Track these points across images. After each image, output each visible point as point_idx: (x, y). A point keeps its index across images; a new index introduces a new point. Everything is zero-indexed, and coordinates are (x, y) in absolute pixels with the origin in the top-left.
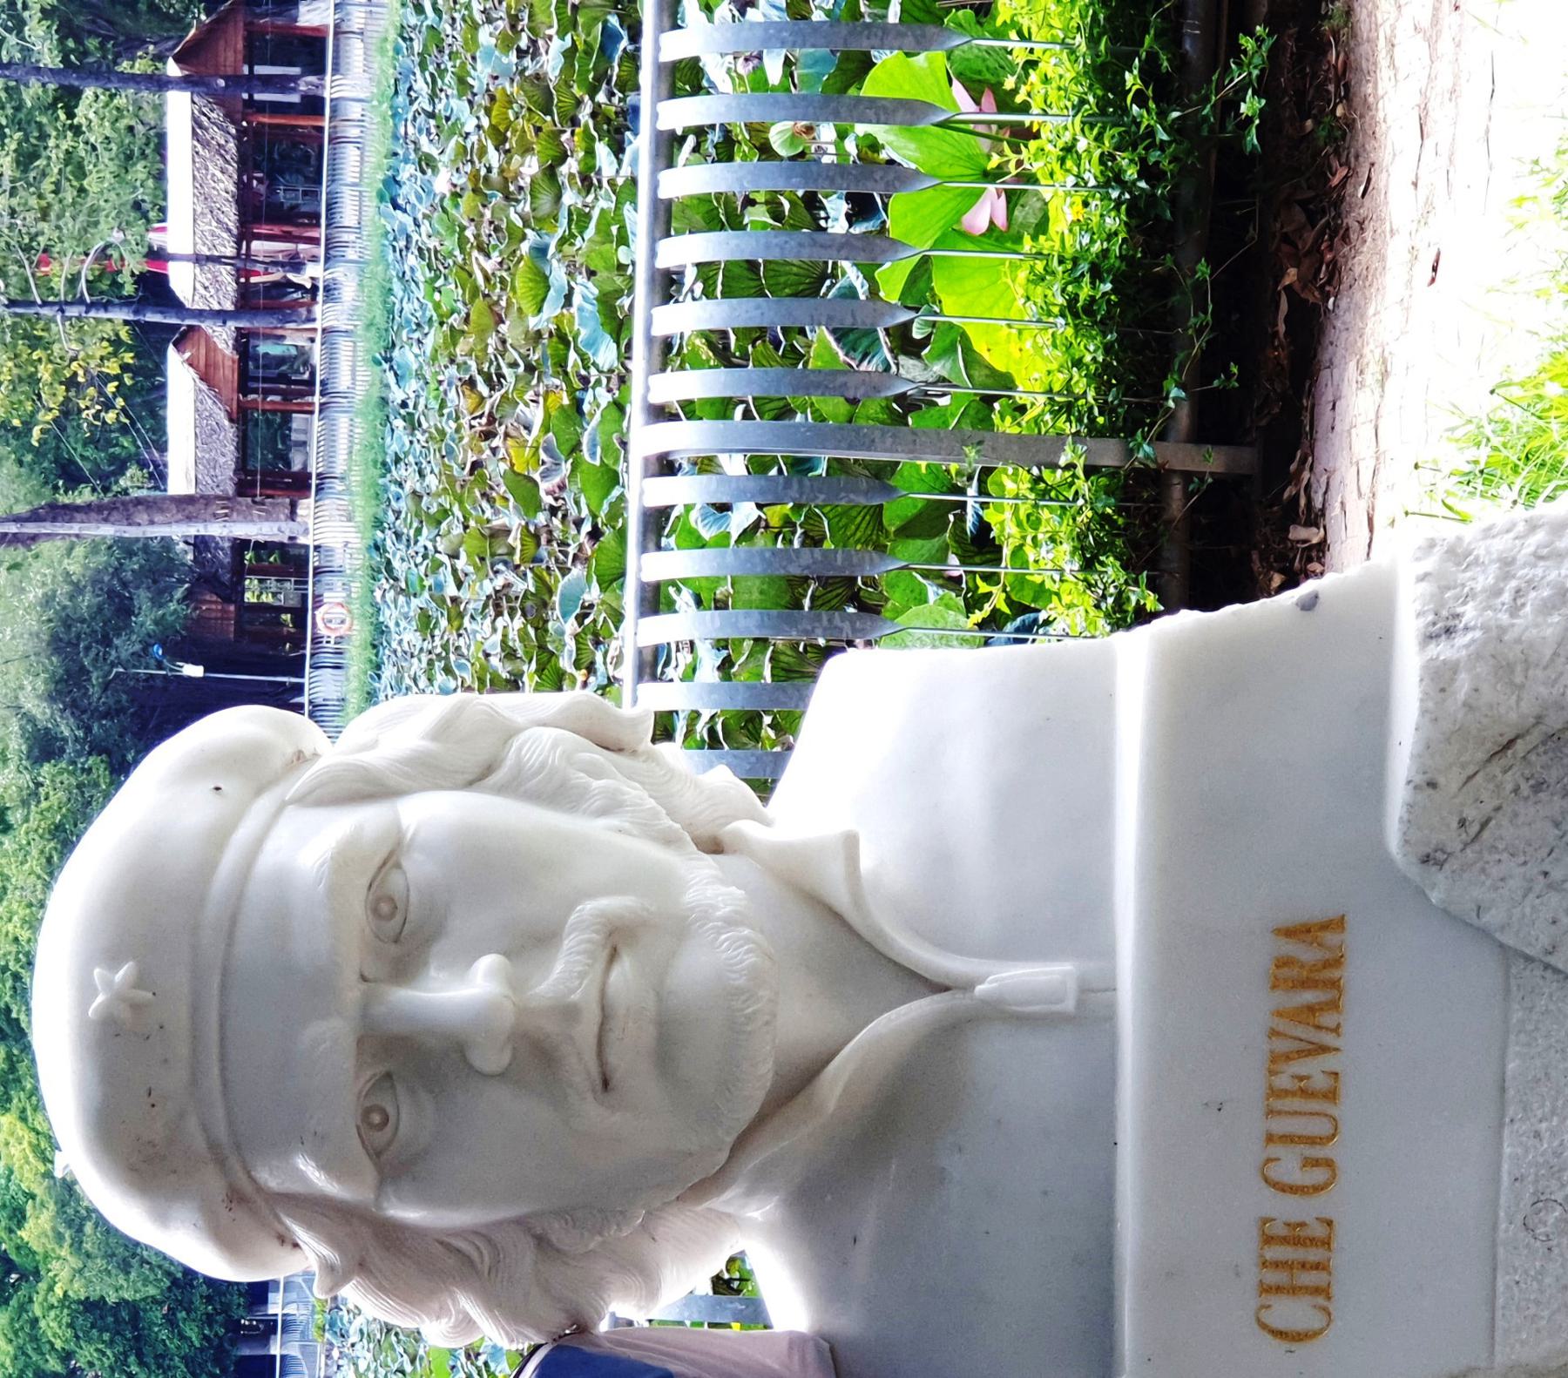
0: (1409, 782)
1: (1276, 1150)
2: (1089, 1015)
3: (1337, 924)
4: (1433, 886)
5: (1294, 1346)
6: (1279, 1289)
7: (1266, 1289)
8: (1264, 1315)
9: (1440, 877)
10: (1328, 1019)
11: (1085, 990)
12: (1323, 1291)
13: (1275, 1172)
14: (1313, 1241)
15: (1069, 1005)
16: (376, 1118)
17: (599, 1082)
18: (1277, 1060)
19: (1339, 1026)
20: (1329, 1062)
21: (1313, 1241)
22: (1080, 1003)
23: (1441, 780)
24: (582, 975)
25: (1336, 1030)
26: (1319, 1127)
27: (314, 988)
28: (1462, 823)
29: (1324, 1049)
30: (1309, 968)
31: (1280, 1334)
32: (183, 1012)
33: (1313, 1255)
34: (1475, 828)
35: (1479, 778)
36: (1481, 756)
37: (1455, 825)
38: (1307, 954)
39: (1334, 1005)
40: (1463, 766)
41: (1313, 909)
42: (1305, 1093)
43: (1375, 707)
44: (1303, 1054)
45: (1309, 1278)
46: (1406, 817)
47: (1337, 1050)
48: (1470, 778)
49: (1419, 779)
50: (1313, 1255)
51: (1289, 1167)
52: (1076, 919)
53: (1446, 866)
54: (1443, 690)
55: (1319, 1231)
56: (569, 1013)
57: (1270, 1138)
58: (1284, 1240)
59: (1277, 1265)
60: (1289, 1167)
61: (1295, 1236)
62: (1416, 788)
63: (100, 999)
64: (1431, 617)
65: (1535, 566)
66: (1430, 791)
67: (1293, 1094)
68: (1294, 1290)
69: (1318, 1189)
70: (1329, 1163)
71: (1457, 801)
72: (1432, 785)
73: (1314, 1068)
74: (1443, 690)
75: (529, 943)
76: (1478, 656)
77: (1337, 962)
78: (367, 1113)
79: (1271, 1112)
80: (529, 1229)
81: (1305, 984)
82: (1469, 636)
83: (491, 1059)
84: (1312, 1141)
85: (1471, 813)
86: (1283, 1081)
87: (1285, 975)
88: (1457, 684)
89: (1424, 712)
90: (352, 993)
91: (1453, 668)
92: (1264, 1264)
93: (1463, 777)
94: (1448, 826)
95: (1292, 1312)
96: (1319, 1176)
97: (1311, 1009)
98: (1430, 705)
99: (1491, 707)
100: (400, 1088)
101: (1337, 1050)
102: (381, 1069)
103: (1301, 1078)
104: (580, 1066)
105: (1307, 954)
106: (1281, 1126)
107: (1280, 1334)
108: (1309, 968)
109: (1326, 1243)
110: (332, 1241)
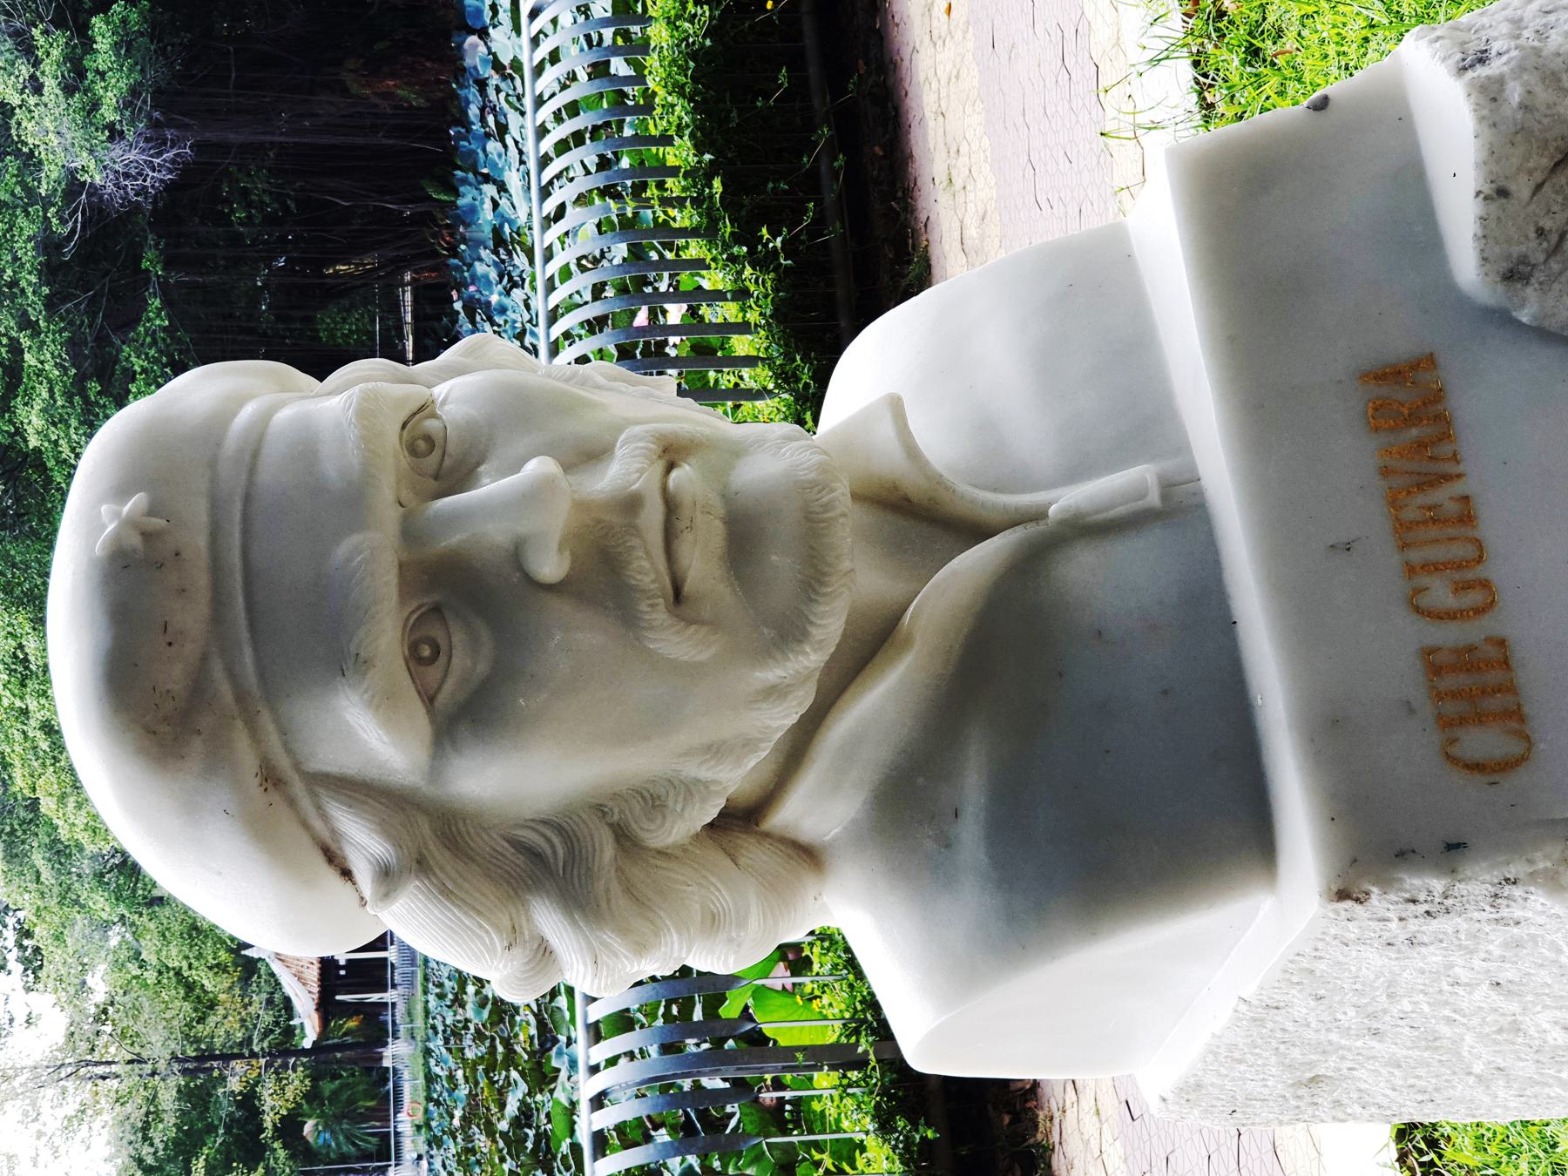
0: (1478, 194)
1: (1425, 580)
2: (1179, 511)
3: (1428, 361)
4: (1523, 303)
5: (1496, 778)
6: (1463, 721)
7: (1446, 723)
8: (1455, 750)
9: (1529, 290)
10: (1445, 449)
11: (1168, 487)
12: (1515, 715)
13: (1425, 601)
14: (1489, 664)
15: (1154, 499)
16: (426, 652)
17: (670, 592)
18: (1394, 502)
19: (1455, 455)
20: (1458, 488)
21: (1489, 664)
22: (1165, 496)
23: (1513, 187)
24: (641, 471)
25: (1455, 458)
26: (1458, 551)
27: (351, 503)
28: (1541, 232)
29: (1448, 478)
30: (1409, 408)
31: (1476, 767)
32: (202, 541)
33: (1494, 677)
34: (1554, 238)
35: (1547, 188)
36: (1546, 162)
37: (1532, 235)
38: (1402, 394)
39: (1446, 436)
40: (1530, 173)
41: (1399, 345)
42: (1434, 521)
43: (1410, 181)
44: (1420, 487)
45: (1495, 703)
46: (1480, 234)
47: (1459, 476)
48: (1539, 187)
49: (1487, 189)
50: (1494, 677)
51: (1440, 593)
52: (1148, 423)
53: (1533, 280)
54: (1494, 100)
55: (1493, 652)
56: (631, 504)
57: (1411, 570)
58: (1455, 668)
59: (1455, 695)
60: (1440, 593)
61: (1467, 659)
62: (1486, 198)
63: (110, 528)
64: (1459, 56)
65: (1545, 25)
66: (1504, 201)
67: (1425, 522)
68: (1480, 718)
69: (1479, 611)
70: (1485, 585)
71: (1532, 207)
72: (1503, 193)
73: (1442, 496)
74: (1494, 100)
75: (587, 454)
76: (1521, 69)
77: (1438, 395)
78: (414, 648)
79: (1404, 546)
80: (605, 814)
81: (1412, 419)
82: (1504, 58)
83: (550, 566)
84: (1458, 566)
85: (1547, 223)
86: (1411, 514)
87: (1382, 416)
88: (1507, 92)
89: (1481, 119)
90: (390, 516)
91: (1500, 81)
92: (1439, 696)
93: (1532, 184)
94: (1527, 237)
95: (1483, 742)
96: (1474, 597)
97: (1421, 445)
98: (1485, 112)
99: (1549, 106)
100: (448, 614)
101: (1459, 476)
102: (428, 600)
103: (1430, 509)
104: (646, 569)
105: (1402, 394)
106: (1415, 556)
107: (1476, 767)
108: (1409, 408)
109: (1505, 663)
110: (386, 832)
